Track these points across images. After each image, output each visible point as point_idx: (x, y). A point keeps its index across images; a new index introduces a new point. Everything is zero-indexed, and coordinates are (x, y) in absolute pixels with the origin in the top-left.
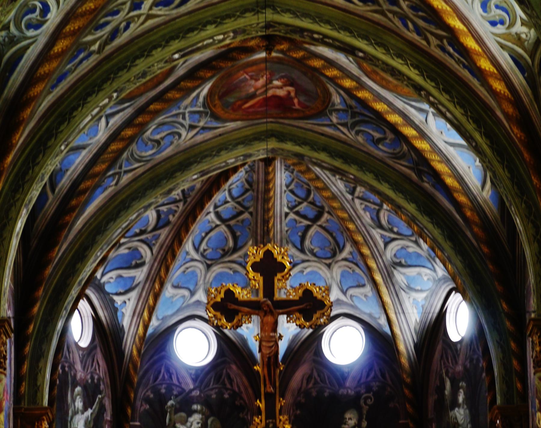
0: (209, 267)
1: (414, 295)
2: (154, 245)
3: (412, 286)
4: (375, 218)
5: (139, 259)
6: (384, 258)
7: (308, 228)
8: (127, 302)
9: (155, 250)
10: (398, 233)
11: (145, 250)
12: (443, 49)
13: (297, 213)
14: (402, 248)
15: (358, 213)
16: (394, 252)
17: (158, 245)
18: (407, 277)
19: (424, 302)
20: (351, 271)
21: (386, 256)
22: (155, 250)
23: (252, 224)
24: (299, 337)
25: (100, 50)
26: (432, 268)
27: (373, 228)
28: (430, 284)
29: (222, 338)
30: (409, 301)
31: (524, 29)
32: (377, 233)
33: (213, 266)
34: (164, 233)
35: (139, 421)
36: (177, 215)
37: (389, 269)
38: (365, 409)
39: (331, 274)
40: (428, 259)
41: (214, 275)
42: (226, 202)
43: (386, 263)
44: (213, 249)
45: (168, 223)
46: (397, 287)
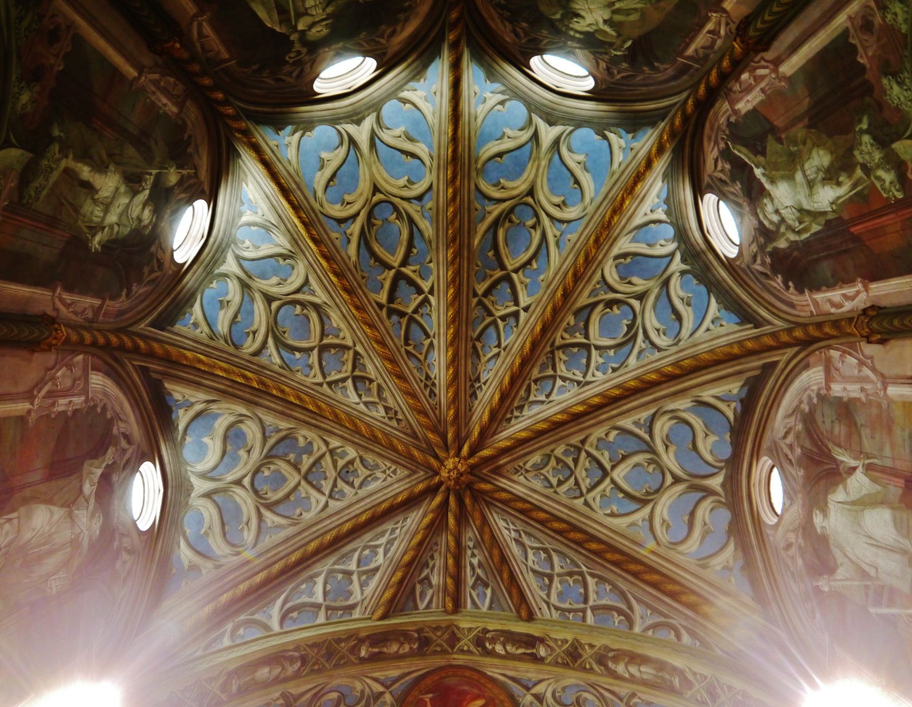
0: (531, 192)
1: (257, 219)
2: (598, 283)
3: (263, 231)
4: (325, 319)
5: (620, 263)
6: (306, 262)
7: (404, 263)
8: (649, 212)
9: (598, 276)
10: (294, 303)
11: (612, 276)
13: (420, 291)
14: (286, 280)
15: (347, 324)
16: (295, 271)
17: (594, 282)
18: (271, 241)
19: (243, 208)
20: (348, 198)
21: (304, 264)
22: (598, 276)
23: (474, 273)
24: (411, 72)
26: (242, 261)
27: (326, 303)
28: (239, 234)
30: (262, 209)
32: (321, 297)
33: (525, 193)
34: (584, 300)
35: (677, 61)
36: (564, 324)
37: (298, 250)
38: (297, 47)
39: (372, 175)
40: (250, 277)
41: (525, 175)
42: (503, 318)
43: (302, 257)
44: (524, 225)
45: (577, 313)
46: (282, 227)
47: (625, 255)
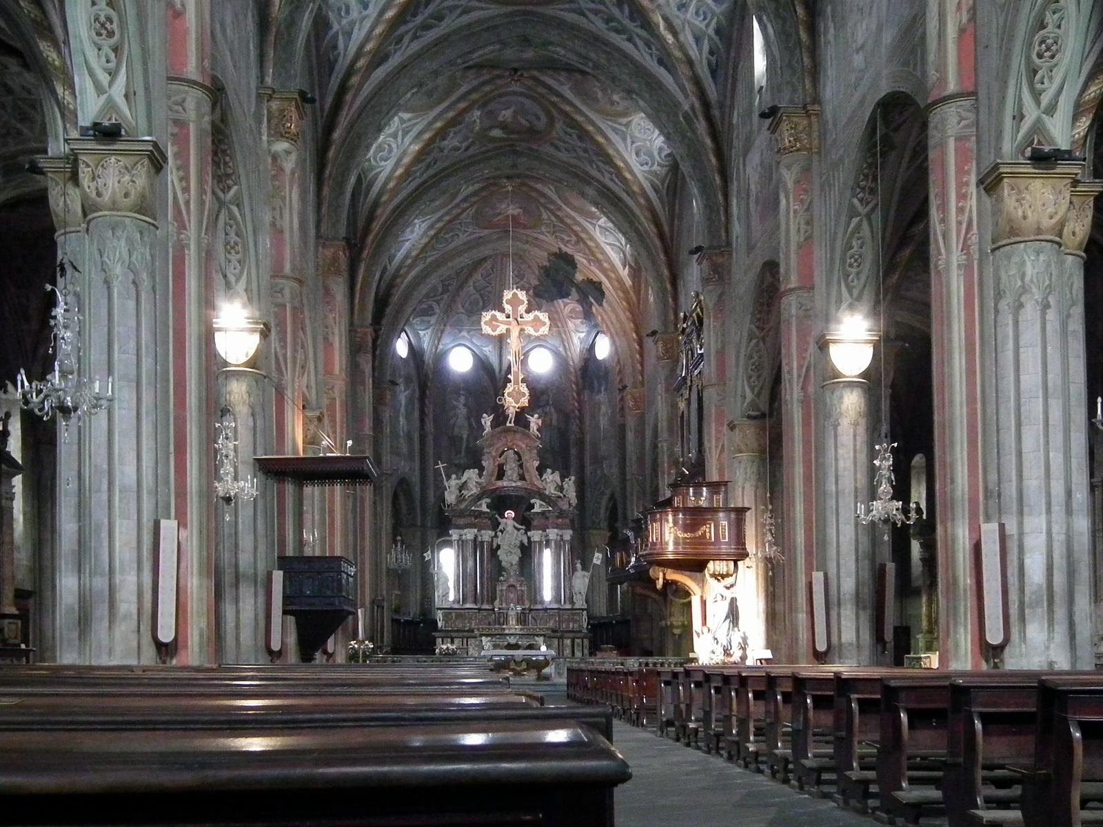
12: (612, 180)
25: (420, 177)
29: (475, 355)
31: (659, 168)
45: (448, 291)
47: (431, 315)
